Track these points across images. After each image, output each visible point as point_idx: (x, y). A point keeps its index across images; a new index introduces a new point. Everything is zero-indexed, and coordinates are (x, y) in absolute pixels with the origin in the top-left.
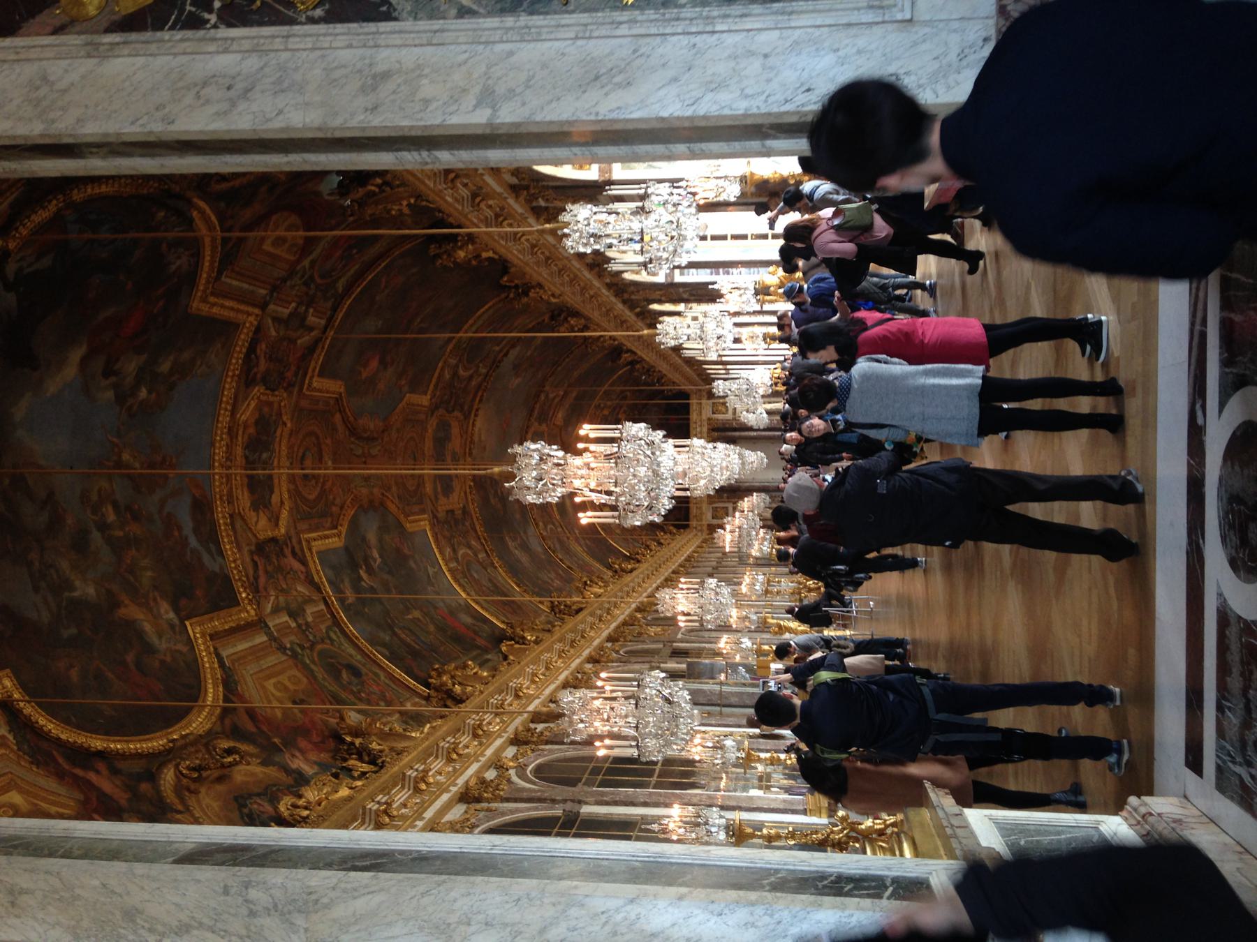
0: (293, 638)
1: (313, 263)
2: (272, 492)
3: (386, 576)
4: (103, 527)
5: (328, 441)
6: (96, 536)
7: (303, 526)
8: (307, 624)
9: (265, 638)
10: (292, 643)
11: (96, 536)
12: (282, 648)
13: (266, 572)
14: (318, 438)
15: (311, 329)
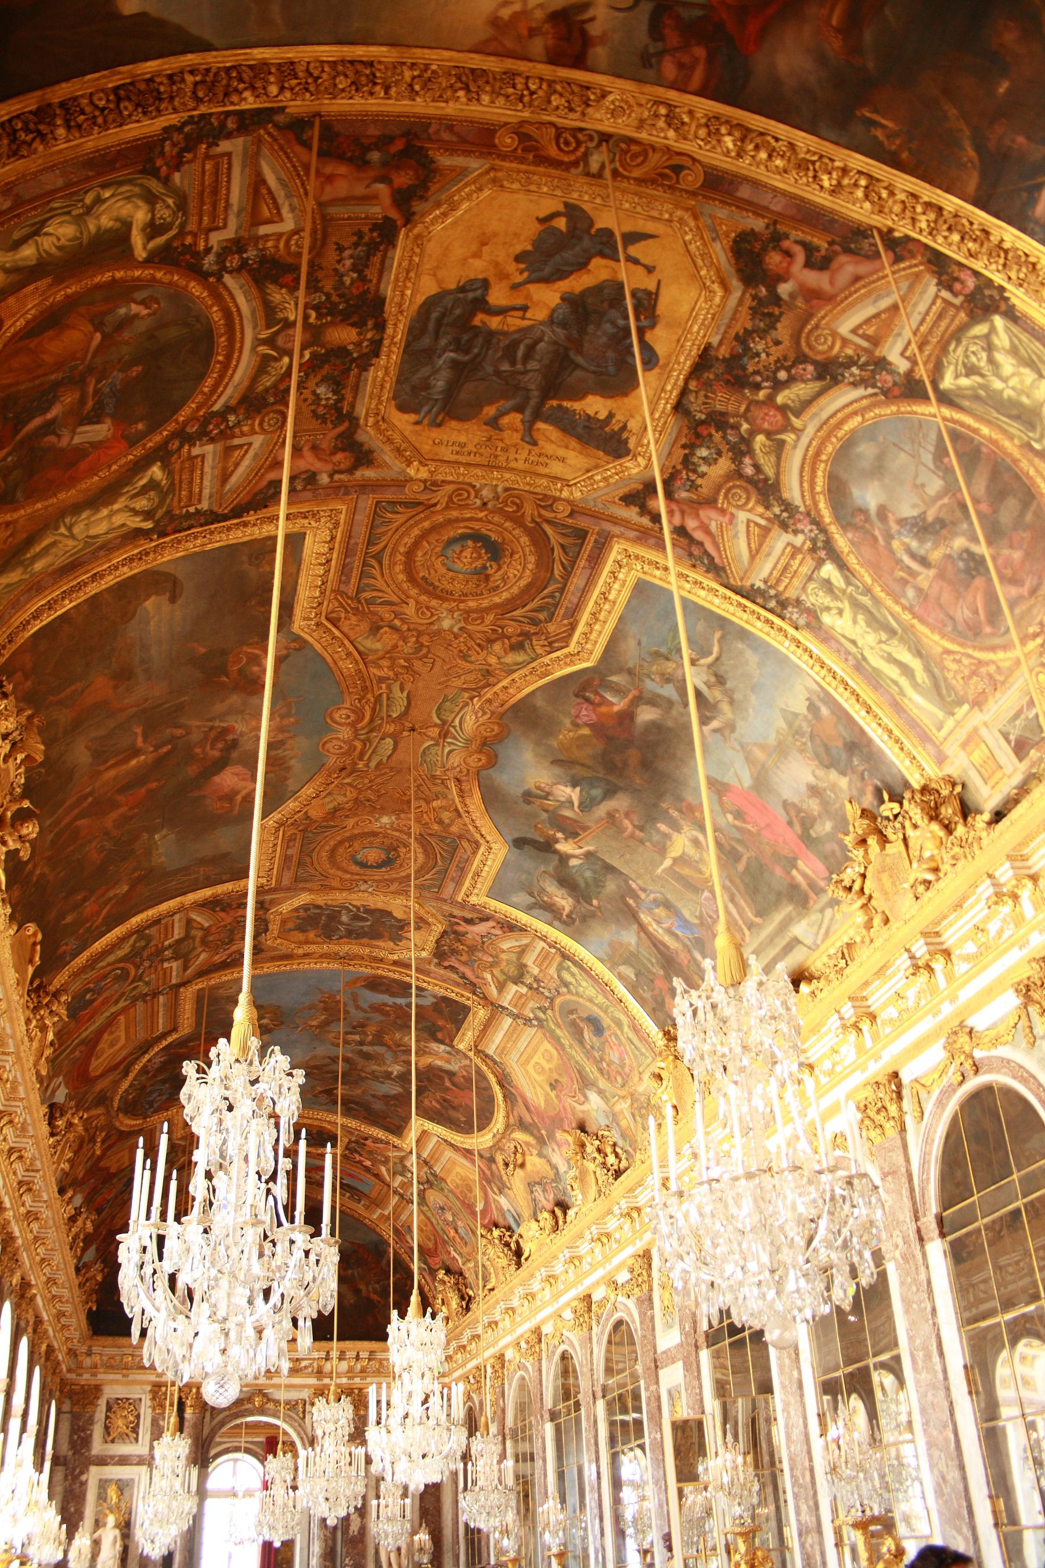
0: (532, 1004)
1: (117, 1002)
2: (389, 914)
3: (601, 811)
4: (362, 1043)
5: (351, 822)
6: (365, 1048)
7: (450, 887)
8: (537, 980)
9: (509, 1020)
10: (532, 1011)
11: (365, 1048)
12: (528, 1021)
13: (465, 963)
14: (341, 843)
15: (189, 922)
